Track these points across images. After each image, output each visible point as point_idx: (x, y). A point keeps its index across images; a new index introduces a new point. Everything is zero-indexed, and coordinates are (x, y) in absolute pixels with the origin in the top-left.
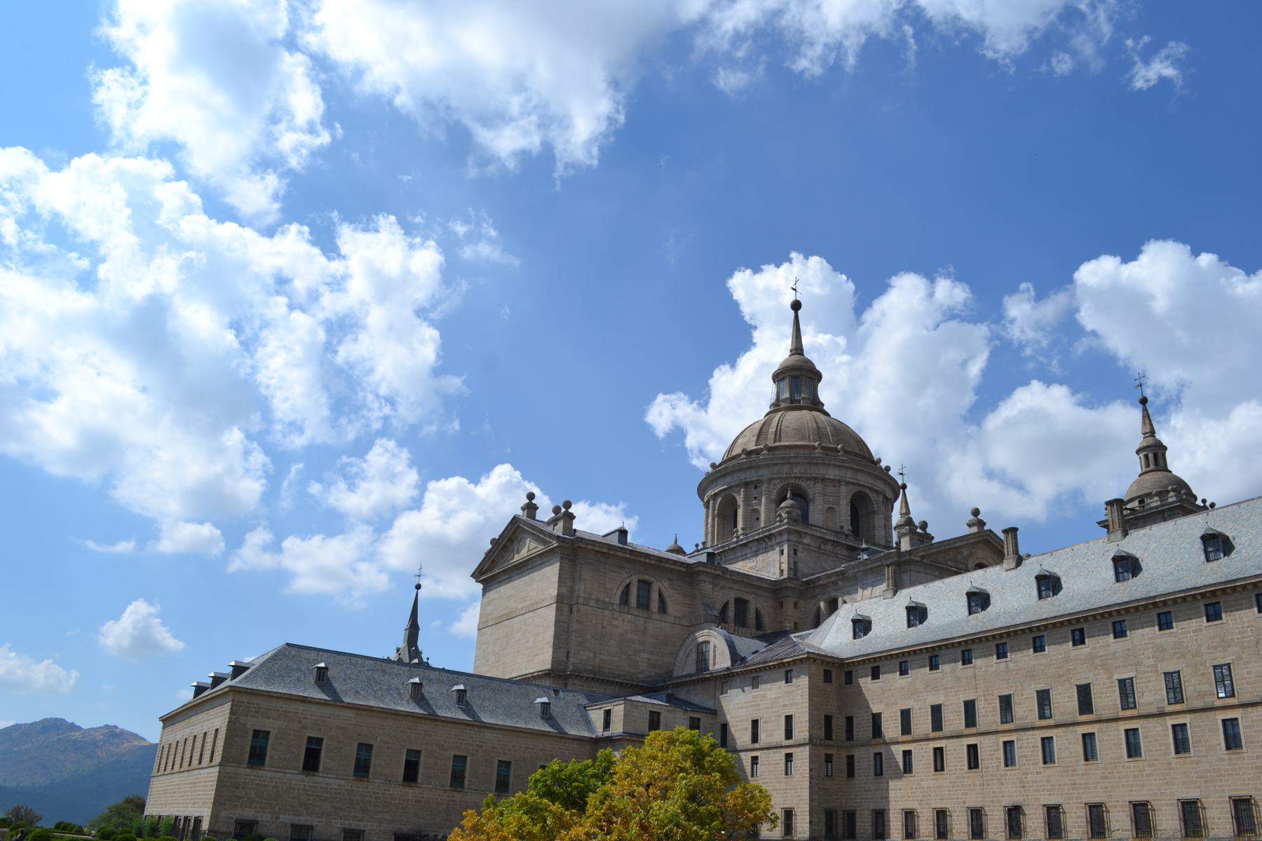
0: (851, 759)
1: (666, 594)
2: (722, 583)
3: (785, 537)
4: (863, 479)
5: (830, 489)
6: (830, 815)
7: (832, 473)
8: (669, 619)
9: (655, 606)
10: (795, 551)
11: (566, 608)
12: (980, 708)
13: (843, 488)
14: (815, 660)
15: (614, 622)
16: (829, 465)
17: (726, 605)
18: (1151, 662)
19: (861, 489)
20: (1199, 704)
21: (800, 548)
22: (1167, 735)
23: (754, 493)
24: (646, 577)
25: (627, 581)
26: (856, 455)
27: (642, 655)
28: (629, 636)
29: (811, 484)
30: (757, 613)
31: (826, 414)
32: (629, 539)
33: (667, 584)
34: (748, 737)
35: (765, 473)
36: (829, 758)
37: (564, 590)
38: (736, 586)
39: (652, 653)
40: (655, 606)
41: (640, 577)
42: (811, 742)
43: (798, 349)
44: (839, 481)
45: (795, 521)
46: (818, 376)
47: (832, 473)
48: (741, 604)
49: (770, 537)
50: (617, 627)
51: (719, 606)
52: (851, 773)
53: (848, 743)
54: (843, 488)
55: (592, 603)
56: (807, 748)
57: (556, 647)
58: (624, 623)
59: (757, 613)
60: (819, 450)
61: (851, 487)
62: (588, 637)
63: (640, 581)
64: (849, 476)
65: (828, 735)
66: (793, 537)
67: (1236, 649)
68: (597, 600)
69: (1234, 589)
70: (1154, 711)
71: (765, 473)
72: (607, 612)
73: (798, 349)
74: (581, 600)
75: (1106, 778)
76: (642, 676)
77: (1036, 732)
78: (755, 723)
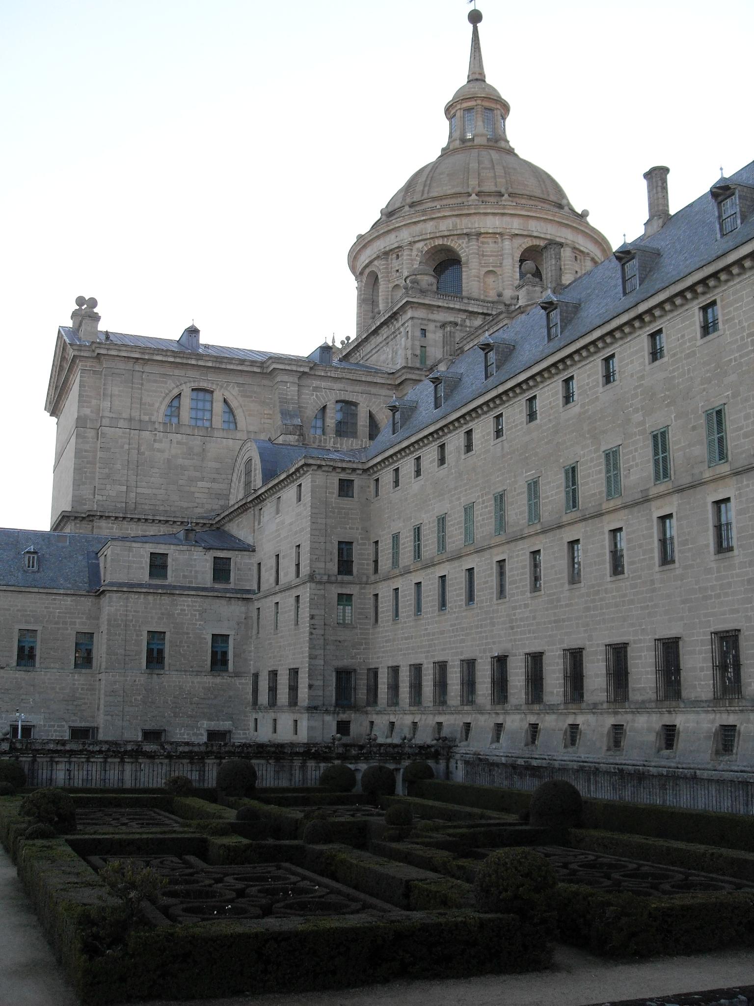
0: (376, 595)
1: (234, 404)
2: (316, 383)
3: (410, 314)
4: (537, 228)
5: (490, 247)
6: (344, 676)
7: (491, 224)
8: (239, 435)
9: (218, 421)
10: (424, 331)
11: (91, 434)
12: (478, 510)
13: (507, 243)
14: (320, 466)
15: (157, 445)
16: (486, 214)
17: (325, 407)
18: (637, 417)
19: (536, 242)
20: (685, 480)
21: (431, 327)
22: (652, 537)
23: (395, 264)
24: (204, 385)
25: (176, 392)
26: (530, 197)
27: (200, 484)
28: (180, 461)
29: (463, 242)
30: (371, 416)
31: (511, 152)
32: (204, 339)
33: (235, 391)
34: (272, 579)
35: (405, 236)
36: (345, 599)
37: (87, 411)
38: (337, 386)
39: (214, 480)
40: (218, 421)
41: (195, 385)
42: (312, 578)
43: (477, 76)
44: (501, 234)
45: (423, 292)
46: (505, 108)
47: (491, 224)
48: (348, 406)
49: (394, 316)
50: (161, 451)
51: (311, 411)
52: (377, 620)
53: (373, 578)
54: (507, 243)
55: (121, 423)
56: (308, 584)
57: (77, 484)
58: (168, 447)
59: (371, 416)
60: (474, 196)
61: (518, 241)
62: (119, 466)
63: (193, 390)
64: (515, 225)
65: (345, 565)
66: (421, 313)
67: (733, 378)
68: (130, 419)
69: (727, 269)
70: (638, 496)
71: (405, 236)
72: (146, 434)
73: (477, 76)
74: (106, 422)
75: (588, 609)
76: (199, 510)
77: (521, 545)
78: (278, 556)
